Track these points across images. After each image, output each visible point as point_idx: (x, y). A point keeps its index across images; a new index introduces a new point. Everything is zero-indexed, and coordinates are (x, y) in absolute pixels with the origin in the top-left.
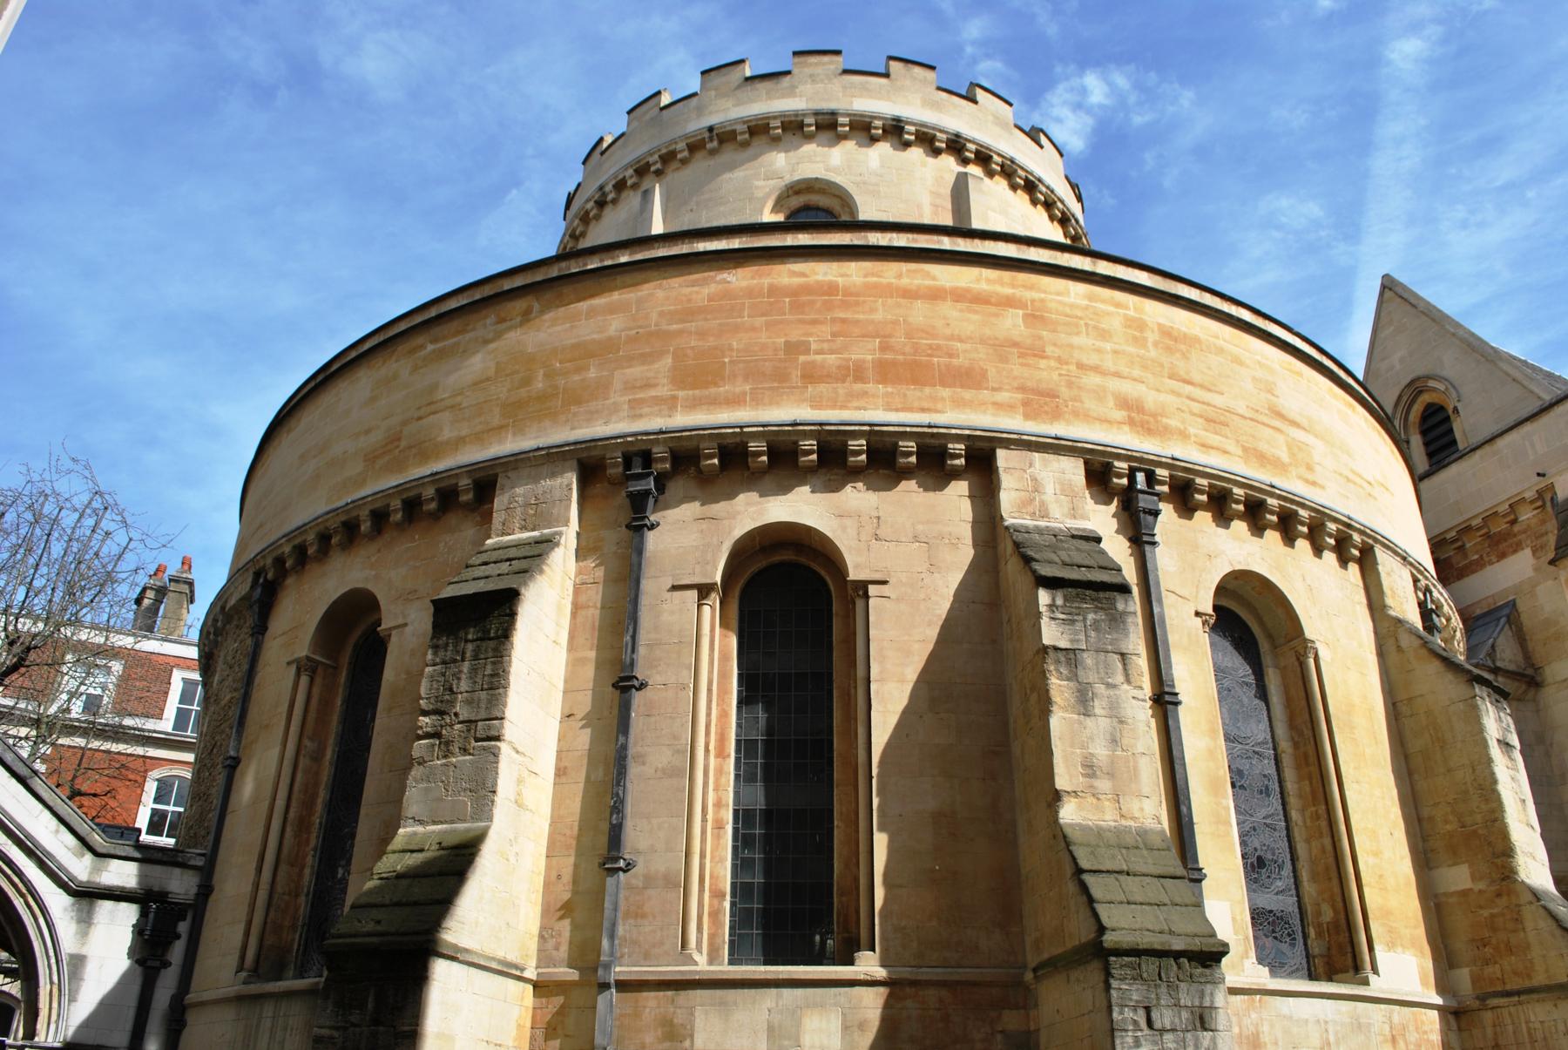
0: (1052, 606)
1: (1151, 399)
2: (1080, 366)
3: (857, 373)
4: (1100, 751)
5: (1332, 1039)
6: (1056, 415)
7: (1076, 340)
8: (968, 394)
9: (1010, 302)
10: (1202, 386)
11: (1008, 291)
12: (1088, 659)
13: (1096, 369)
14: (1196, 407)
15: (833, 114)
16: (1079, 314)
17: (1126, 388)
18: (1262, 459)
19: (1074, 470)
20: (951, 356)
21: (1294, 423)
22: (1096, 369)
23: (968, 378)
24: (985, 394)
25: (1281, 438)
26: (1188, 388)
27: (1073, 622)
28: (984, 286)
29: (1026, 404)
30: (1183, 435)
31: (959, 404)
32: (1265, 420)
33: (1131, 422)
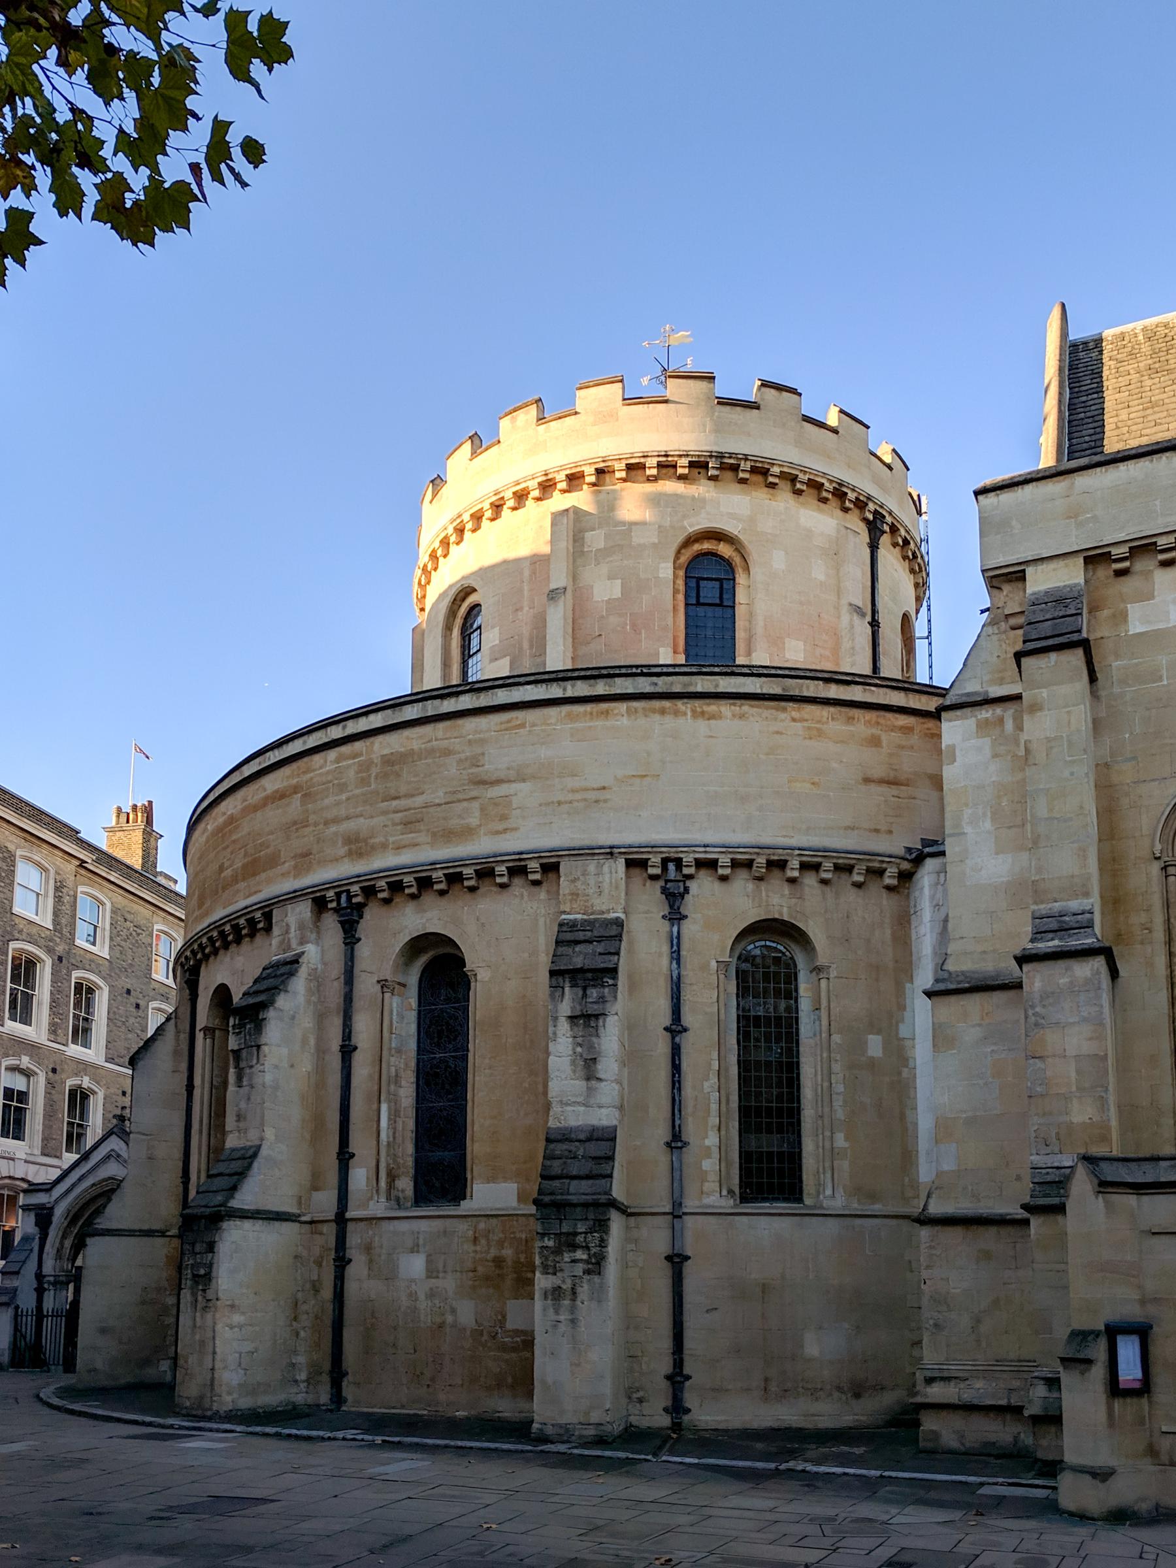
0: (234, 1026)
4: (243, 1105)
6: (308, 869)
7: (326, 801)
12: (244, 1054)
13: (336, 821)
16: (330, 778)
17: (346, 826)
18: (449, 836)
20: (268, 847)
21: (499, 782)
22: (336, 821)
25: (476, 805)
26: (395, 803)
27: (240, 1033)
29: (295, 867)
30: (384, 846)
32: (461, 796)
33: (350, 854)
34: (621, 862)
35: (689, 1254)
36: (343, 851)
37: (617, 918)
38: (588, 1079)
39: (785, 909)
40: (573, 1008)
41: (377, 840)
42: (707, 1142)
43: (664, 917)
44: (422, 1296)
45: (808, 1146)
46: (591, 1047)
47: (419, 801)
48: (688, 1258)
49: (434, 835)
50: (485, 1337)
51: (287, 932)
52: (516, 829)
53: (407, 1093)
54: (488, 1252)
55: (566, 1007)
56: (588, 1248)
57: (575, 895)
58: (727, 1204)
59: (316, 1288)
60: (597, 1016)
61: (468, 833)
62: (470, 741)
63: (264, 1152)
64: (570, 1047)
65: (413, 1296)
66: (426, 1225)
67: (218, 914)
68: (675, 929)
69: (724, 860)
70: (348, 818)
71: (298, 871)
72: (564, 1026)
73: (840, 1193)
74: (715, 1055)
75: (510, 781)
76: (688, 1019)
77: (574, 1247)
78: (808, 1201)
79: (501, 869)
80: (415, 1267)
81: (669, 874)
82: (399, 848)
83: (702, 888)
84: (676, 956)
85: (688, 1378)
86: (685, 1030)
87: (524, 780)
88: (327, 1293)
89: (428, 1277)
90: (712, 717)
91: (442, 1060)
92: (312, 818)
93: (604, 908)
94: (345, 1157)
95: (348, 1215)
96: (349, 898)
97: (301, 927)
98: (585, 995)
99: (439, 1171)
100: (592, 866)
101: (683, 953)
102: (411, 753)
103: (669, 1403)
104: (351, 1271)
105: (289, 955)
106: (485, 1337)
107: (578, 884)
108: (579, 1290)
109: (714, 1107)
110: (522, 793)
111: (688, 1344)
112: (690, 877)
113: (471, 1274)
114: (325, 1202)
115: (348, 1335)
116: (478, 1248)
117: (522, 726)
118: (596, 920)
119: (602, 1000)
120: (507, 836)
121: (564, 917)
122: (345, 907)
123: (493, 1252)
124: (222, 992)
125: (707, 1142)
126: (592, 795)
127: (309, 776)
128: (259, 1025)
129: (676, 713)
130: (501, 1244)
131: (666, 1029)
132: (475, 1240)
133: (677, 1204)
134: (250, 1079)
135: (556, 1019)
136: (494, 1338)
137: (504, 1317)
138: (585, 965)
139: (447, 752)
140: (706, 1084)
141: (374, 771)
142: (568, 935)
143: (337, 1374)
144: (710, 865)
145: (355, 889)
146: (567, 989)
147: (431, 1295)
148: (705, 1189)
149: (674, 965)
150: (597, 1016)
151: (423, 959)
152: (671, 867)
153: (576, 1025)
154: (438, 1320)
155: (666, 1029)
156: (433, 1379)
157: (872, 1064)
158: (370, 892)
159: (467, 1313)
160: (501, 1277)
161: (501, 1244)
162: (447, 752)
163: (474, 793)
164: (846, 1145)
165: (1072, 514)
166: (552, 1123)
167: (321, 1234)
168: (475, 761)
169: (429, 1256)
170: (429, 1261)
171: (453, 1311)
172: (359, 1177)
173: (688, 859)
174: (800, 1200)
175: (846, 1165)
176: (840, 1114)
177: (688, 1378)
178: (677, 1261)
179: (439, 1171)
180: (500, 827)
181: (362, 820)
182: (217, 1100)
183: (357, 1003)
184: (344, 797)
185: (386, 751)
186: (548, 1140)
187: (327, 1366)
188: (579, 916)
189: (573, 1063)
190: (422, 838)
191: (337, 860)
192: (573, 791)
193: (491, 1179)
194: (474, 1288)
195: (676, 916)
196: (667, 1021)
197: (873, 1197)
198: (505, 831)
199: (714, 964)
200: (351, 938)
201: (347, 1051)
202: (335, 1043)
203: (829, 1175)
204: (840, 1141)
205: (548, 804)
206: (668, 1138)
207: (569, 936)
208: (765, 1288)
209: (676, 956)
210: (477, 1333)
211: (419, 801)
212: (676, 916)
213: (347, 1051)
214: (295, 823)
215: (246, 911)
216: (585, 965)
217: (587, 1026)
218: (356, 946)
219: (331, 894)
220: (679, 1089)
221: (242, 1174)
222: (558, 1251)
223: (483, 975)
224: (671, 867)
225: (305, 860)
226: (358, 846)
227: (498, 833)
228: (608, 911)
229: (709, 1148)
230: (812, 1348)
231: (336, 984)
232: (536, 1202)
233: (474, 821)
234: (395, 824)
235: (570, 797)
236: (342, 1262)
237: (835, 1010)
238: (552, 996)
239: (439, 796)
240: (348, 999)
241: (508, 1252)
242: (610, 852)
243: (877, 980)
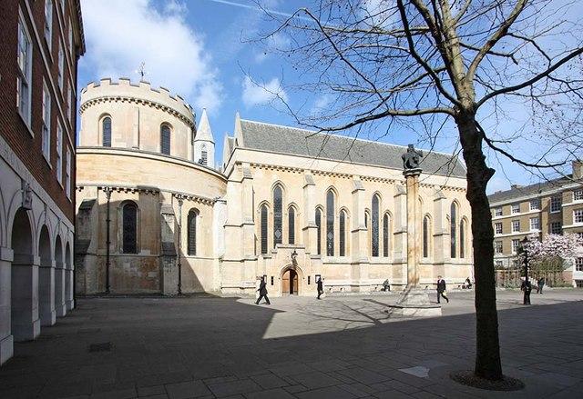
53: (121, 230)
59: (100, 269)
66: (129, 256)
80: (127, 265)
83: (185, 201)
88: (104, 270)
94: (108, 243)
99: (130, 245)
114: (103, 252)
115: (110, 279)
143: (107, 287)
144: (185, 197)
158: (114, 189)
179: (130, 245)
201: (108, 221)
202: (104, 219)
213: (108, 221)
236: (108, 264)
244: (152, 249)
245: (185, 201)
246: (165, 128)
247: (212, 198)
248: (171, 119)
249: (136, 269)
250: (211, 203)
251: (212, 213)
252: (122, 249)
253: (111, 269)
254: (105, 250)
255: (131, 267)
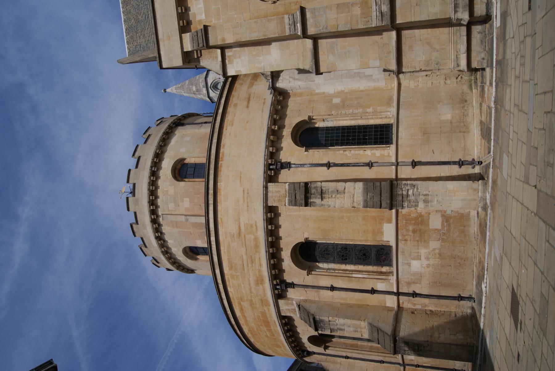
0: (322, 331)
1: (252, 279)
2: (251, 292)
3: (270, 330)
4: (352, 329)
5: (406, 262)
6: (267, 300)
7: (244, 292)
8: (268, 316)
9: (240, 304)
10: (243, 261)
11: (237, 304)
12: (332, 327)
13: (250, 289)
14: (250, 265)
15: (162, 252)
18: (257, 246)
19: (281, 302)
21: (239, 228)
22: (250, 289)
23: (264, 315)
24: (267, 312)
25: (247, 236)
26: (245, 266)
28: (238, 308)
29: (266, 306)
30: (260, 271)
31: (271, 316)
32: (244, 242)
34: (269, 184)
35: (411, 160)
36: (261, 287)
37: (289, 185)
38: (344, 193)
39: (289, 130)
40: (319, 198)
41: (257, 273)
42: (370, 154)
43: (289, 170)
44: (428, 262)
45: (372, 122)
46: (332, 192)
47: (245, 257)
48: (413, 160)
49: (256, 252)
50: (444, 237)
51: (289, 310)
52: (256, 222)
54: (411, 236)
55: (318, 201)
56: (408, 190)
57: (279, 200)
58: (393, 147)
60: (322, 190)
61: (256, 239)
62: (226, 238)
63: (370, 321)
64: (333, 199)
65: (428, 266)
67: (282, 338)
68: (293, 166)
69: (271, 149)
70: (250, 284)
71: (268, 305)
72: (325, 202)
73: (389, 109)
74: (338, 152)
75: (239, 224)
76: (325, 162)
77: (408, 195)
78: (392, 121)
79: (270, 227)
81: (274, 168)
82: (261, 265)
84: (302, 165)
85: (460, 160)
86: (329, 162)
87: (239, 219)
89: (420, 259)
90: (223, 155)
91: (338, 254)
92: (249, 298)
93: (284, 190)
94: (373, 291)
95: (395, 291)
96: (277, 284)
97: (287, 304)
98: (314, 194)
99: (378, 255)
100: (270, 195)
101: (301, 163)
102: (229, 259)
103: (470, 166)
104: (418, 291)
105: (297, 309)
106: (444, 237)
107: (276, 199)
108: (425, 193)
109: (357, 152)
110: (244, 220)
111: (446, 160)
112: (275, 161)
113: (419, 242)
116: (409, 239)
117: (221, 219)
118: (289, 193)
119: (316, 188)
120: (258, 225)
121: (287, 204)
122: (281, 288)
123: (411, 233)
124: (312, 339)
125: (370, 154)
126: (246, 195)
127: (235, 298)
128: (322, 321)
129: (221, 166)
130: (407, 230)
131: (328, 169)
132: (406, 240)
133: (392, 164)
134: (341, 325)
135: (322, 205)
136: (444, 234)
137: (436, 230)
138: (305, 194)
139: (229, 246)
140: (348, 155)
141: (234, 273)
142: (294, 202)
145: (275, 282)
146: (312, 200)
147: (427, 258)
148: (387, 155)
149: (306, 166)
150: (322, 190)
151: (301, 259)
152: (271, 167)
153: (325, 198)
154: (437, 256)
155: (328, 169)
156: (462, 259)
157: (343, 101)
159: (434, 244)
160: (420, 230)
161: (407, 230)
162: (229, 246)
163: (243, 236)
164: (371, 108)
165: (169, 38)
166: (361, 206)
167: (403, 303)
168: (233, 236)
169: (412, 259)
170: (414, 259)
171: (434, 250)
172: (380, 286)
173: (270, 161)
174: (392, 125)
175: (378, 108)
176: (360, 110)
177: (460, 160)
178: (414, 164)
180: (255, 227)
181: (250, 279)
182: (351, 347)
183: (316, 285)
184: (242, 285)
185: (228, 269)
186: (367, 207)
187: (456, 302)
188: (287, 199)
189: (338, 198)
190: (257, 256)
191: (264, 289)
192: (244, 201)
193: (382, 233)
194: (425, 241)
195: (288, 165)
196: (325, 168)
197: (391, 99)
198: (256, 226)
199: (306, 153)
200: (292, 285)
201: (332, 288)
203: (382, 114)
204: (370, 110)
205: (248, 210)
206: (368, 167)
207: (293, 202)
208: (425, 133)
209: (302, 165)
210: (443, 241)
211: (245, 257)
212: (288, 165)
213: (332, 288)
214: (251, 305)
215: (283, 325)
216: (305, 194)
217: (325, 193)
218: (295, 283)
219: (276, 292)
220: (350, 164)
221: (378, 330)
222: (410, 201)
223: (306, 236)
224: (271, 167)
225: (264, 302)
226: (259, 281)
227: (257, 229)
228: (286, 189)
229: (372, 154)
230: (448, 117)
231: (308, 292)
232: (391, 209)
233: (252, 237)
234: (252, 266)
235: (246, 202)
236: (415, 295)
237: (324, 113)
238: (314, 206)
239: (243, 250)
240: (314, 287)
241: (411, 228)
242: (266, 188)
243: (314, 101)
244: (381, 221)
245: (284, 157)
246: (181, 171)
247: (269, 97)
248: (167, 165)
249: (423, 252)
250: (281, 97)
251: (301, 95)
252: (385, 269)
253: (425, 292)
254: (388, 297)
255: (419, 258)
